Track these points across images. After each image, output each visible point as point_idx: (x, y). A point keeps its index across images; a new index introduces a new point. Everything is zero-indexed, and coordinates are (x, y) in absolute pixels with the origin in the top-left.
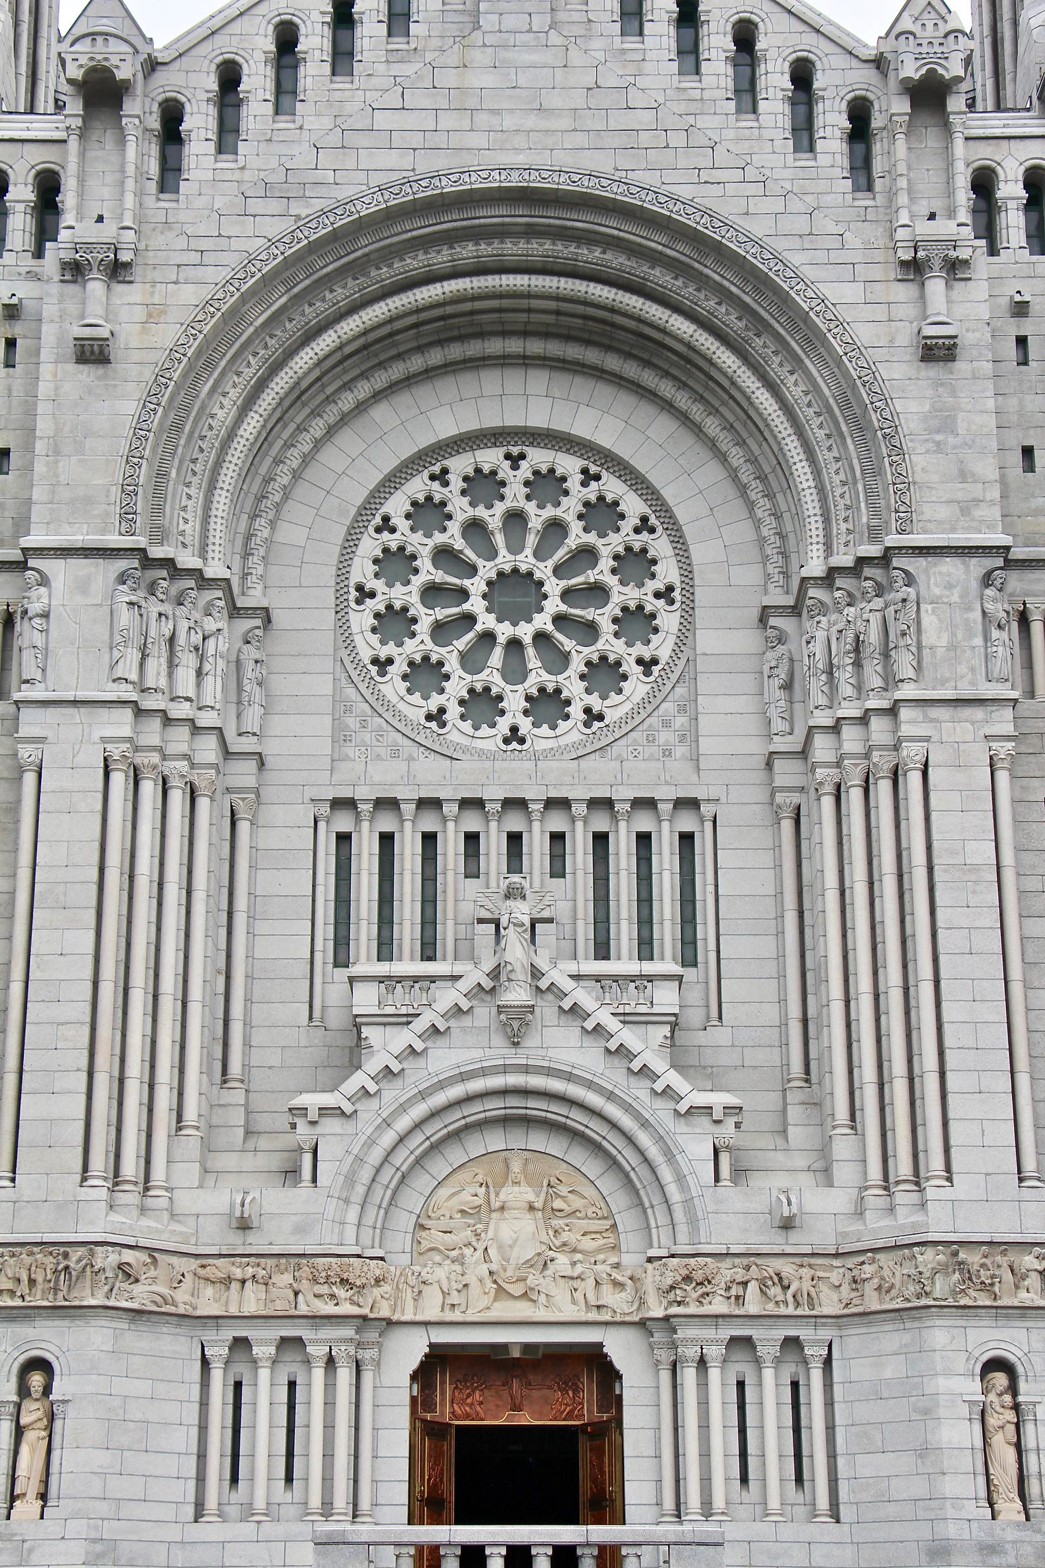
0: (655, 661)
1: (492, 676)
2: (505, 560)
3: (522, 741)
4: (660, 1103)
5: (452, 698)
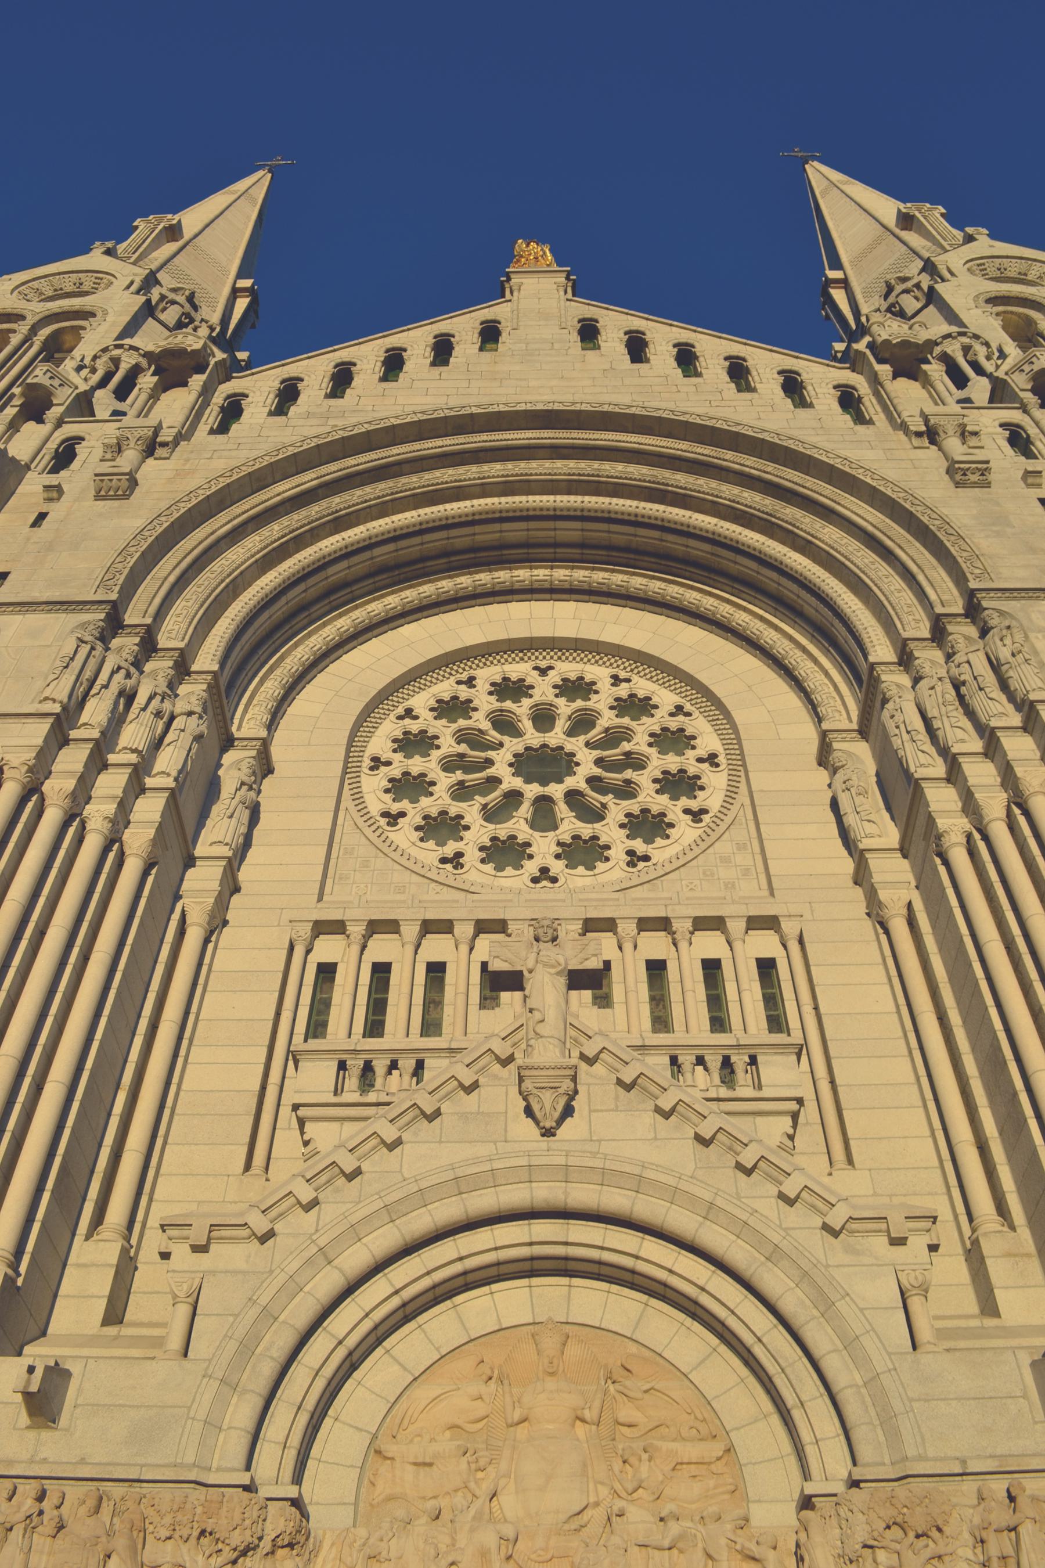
0: (704, 811)
1: (518, 825)
2: (533, 738)
3: (554, 880)
4: (793, 1216)
5: (471, 844)
